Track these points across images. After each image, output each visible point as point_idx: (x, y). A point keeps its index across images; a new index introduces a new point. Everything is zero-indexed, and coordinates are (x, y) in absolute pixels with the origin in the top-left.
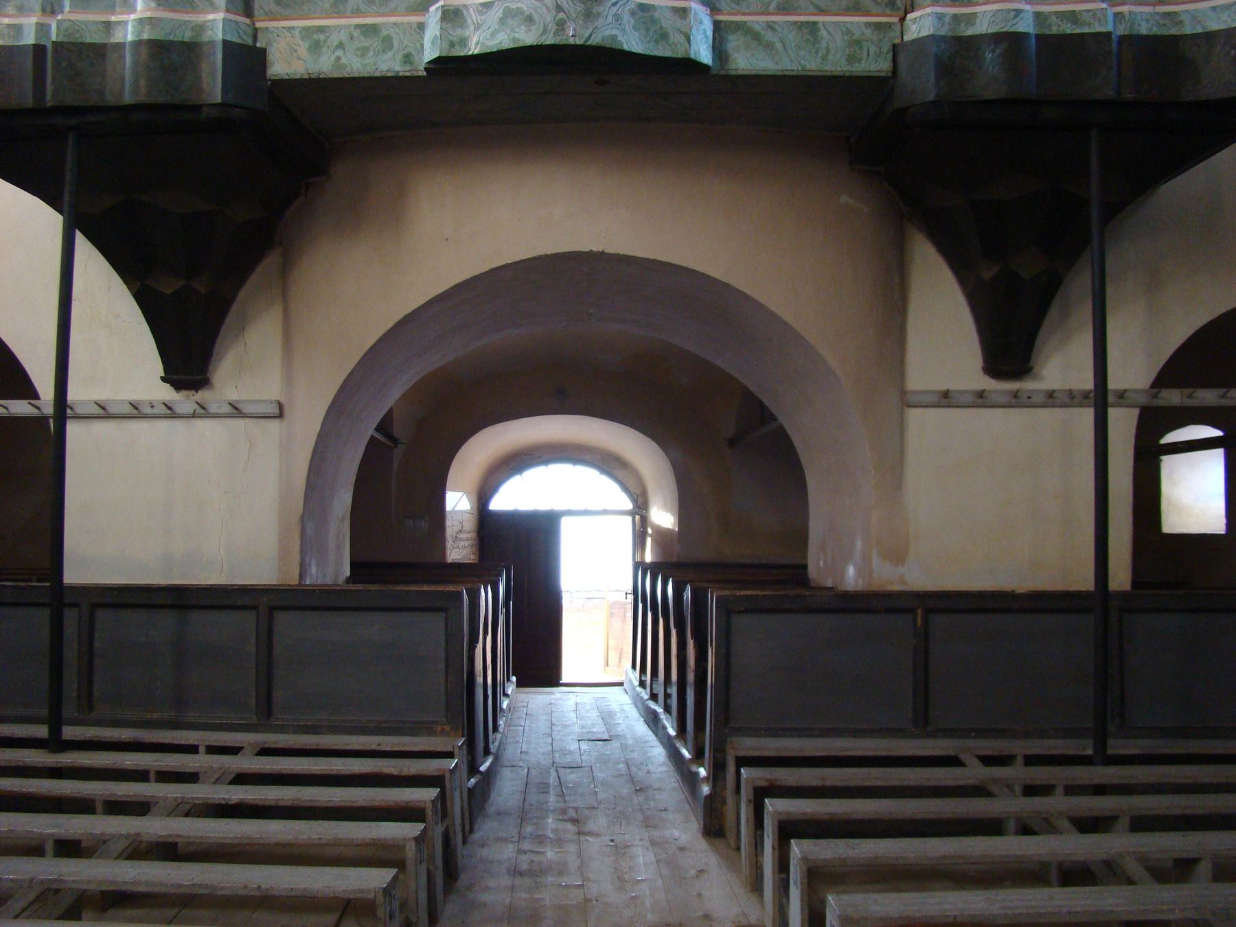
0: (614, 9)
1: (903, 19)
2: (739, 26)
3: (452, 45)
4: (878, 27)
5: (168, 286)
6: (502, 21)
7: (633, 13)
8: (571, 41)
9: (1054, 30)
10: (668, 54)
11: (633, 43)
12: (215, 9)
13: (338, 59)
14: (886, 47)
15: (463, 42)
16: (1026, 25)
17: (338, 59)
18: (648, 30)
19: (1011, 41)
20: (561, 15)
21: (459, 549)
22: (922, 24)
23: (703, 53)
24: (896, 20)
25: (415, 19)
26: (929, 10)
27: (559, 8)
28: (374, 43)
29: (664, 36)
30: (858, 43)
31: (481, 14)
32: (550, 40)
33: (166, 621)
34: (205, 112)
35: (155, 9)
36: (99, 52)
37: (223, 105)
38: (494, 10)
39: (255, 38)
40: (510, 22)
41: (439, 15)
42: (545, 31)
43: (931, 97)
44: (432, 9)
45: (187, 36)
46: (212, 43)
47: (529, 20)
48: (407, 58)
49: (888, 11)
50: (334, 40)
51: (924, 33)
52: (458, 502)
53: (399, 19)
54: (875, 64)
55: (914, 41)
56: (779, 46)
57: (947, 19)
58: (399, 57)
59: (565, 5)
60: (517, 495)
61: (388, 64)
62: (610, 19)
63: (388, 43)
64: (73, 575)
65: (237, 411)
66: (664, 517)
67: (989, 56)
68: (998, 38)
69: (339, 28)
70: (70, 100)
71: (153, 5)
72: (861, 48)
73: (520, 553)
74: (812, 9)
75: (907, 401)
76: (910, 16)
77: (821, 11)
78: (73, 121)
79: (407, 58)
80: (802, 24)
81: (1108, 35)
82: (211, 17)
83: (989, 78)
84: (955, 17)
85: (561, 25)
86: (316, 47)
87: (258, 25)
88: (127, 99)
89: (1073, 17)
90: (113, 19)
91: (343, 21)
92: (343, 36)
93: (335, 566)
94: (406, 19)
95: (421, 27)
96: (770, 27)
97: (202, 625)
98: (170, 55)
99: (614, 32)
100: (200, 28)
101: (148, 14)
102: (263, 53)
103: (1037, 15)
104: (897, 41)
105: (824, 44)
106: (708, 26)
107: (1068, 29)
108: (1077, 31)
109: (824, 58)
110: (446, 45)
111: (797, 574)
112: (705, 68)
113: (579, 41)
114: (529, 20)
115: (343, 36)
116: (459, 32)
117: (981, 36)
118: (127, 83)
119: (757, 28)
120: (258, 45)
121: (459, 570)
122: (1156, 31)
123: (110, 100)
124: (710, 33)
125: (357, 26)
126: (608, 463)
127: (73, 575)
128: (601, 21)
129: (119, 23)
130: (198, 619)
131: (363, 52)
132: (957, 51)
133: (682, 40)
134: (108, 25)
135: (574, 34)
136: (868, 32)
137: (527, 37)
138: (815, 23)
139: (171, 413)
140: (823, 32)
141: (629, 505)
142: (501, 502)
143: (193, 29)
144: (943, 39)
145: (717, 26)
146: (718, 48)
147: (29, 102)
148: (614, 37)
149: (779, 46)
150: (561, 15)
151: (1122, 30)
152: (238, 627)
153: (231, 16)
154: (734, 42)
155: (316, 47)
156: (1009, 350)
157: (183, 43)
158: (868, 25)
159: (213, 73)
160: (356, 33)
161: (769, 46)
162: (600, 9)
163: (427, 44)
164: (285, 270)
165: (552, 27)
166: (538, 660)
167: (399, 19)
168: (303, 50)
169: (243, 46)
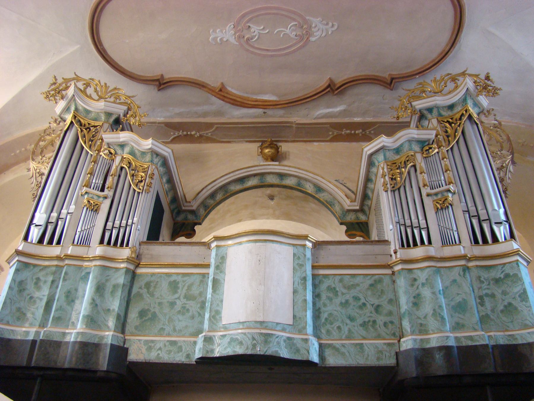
0: (277, 339)
1: (399, 341)
2: (330, 345)
3: (207, 352)
4: (389, 345)
6: (229, 343)
7: (285, 341)
8: (259, 353)
9: (464, 344)
10: (300, 358)
11: (285, 354)
12: (109, 330)
13: (159, 354)
14: (393, 353)
15: (212, 351)
16: (451, 343)
17: (159, 354)
18: (291, 348)
19: (446, 350)
20: (255, 342)
22: (408, 343)
23: (315, 359)
24: (396, 341)
25: (193, 339)
26: (410, 337)
27: (254, 339)
28: (174, 349)
29: (298, 351)
30: (381, 352)
31: (221, 339)
32: (249, 352)
34: (98, 374)
35: (85, 329)
36: (58, 345)
37: (107, 371)
38: (226, 338)
39: (124, 343)
40: (233, 343)
41: (203, 339)
42: (247, 348)
43: (414, 375)
44: (200, 336)
45: (96, 341)
46: (106, 344)
47: (241, 343)
48: (188, 356)
49: (393, 338)
50: (158, 346)
51: (409, 347)
53: (186, 339)
54: (390, 361)
55: (406, 351)
56: (347, 354)
57: (418, 341)
58: (185, 355)
59: (256, 337)
61: (179, 358)
62: (275, 344)
63: (180, 349)
67: (438, 357)
68: (441, 348)
69: (160, 341)
70: (42, 364)
71: (84, 327)
72: (382, 354)
74: (361, 338)
76: (402, 340)
77: (364, 338)
78: (42, 373)
79: (188, 356)
80: (357, 344)
81: (487, 346)
82: (107, 333)
83: (439, 366)
84: (421, 340)
85: (254, 346)
86: (150, 349)
87: (126, 337)
88: (66, 366)
89: (471, 338)
90: (67, 331)
91: (162, 339)
92: (161, 345)
94: (189, 339)
95: (195, 343)
96: (343, 345)
98: (88, 348)
99: (277, 349)
100: (102, 338)
101: (82, 331)
102: (127, 349)
103: (456, 338)
104: (398, 351)
105: (366, 353)
106: (316, 346)
107: (470, 343)
108: (473, 344)
109: (367, 359)
110: (205, 352)
112: (315, 364)
113: (262, 353)
114: (241, 343)
115: (161, 345)
116: (211, 347)
117: (433, 348)
118: (67, 359)
119: (337, 346)
120: (125, 346)
122: (507, 342)
123: (59, 365)
124: (318, 349)
125: (168, 341)
128: (271, 345)
129: (69, 333)
131: (170, 352)
132: (424, 355)
133: (306, 352)
134: (64, 334)
135: (259, 350)
136: (385, 347)
137: (240, 350)
138: (362, 344)
140: (366, 347)
143: (99, 338)
144: (418, 349)
145: (321, 345)
146: (321, 356)
147: (24, 364)
148: (277, 352)
149: (347, 354)
150: (255, 342)
151: (492, 343)
153: (116, 334)
154: (328, 352)
155: (150, 349)
157: (94, 344)
158: (385, 344)
159: (105, 357)
160: (167, 344)
161: (343, 354)
162: (271, 339)
163: (197, 351)
165: (250, 347)
167: (186, 339)
168: (144, 350)
169: (119, 346)
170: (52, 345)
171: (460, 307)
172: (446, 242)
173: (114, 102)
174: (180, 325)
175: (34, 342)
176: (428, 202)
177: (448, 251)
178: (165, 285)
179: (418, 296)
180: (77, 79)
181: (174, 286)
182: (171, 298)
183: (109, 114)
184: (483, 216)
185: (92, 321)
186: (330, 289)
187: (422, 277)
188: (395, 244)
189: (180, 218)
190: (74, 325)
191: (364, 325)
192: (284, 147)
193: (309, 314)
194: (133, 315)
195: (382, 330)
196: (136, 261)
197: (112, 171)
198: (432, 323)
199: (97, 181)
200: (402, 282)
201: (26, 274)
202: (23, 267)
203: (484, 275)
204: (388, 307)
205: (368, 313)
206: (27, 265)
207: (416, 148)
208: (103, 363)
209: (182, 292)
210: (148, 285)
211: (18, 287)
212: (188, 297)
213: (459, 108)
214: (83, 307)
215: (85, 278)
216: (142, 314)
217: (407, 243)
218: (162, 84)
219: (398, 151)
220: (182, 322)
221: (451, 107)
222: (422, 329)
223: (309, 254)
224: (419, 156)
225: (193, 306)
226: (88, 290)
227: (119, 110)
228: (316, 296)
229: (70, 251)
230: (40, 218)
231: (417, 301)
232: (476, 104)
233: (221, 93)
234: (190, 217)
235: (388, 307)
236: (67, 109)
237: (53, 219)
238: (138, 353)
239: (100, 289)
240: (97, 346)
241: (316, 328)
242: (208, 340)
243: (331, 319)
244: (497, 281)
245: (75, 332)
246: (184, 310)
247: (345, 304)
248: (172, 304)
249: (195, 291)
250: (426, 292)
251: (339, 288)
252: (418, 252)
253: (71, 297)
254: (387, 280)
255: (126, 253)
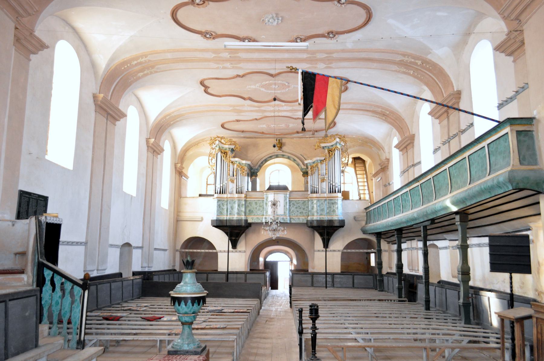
5: (233, 238)
16: (319, 219)
19: (317, 221)
21: (261, 267)
22: (309, 218)
33: (235, 275)
36: (232, 220)
52: (261, 259)
60: (270, 258)
64: (219, 270)
65: (240, 252)
66: (295, 262)
73: (271, 267)
75: (314, 251)
83: (315, 224)
93: (249, 270)
97: (239, 275)
98: (239, 221)
111: (308, 271)
121: (262, 270)
126: (286, 253)
127: (219, 270)
130: (238, 275)
132: (312, 221)
139: (232, 252)
141: (289, 260)
142: (267, 260)
146: (290, 220)
152: (243, 276)
154: (292, 220)
156: (326, 245)
164: (246, 235)
166: (274, 285)
170: (231, 221)
171: (322, 210)
172: (323, 192)
173: (230, 145)
174: (258, 213)
175: (227, 220)
176: (320, 180)
177: (322, 195)
178: (254, 203)
179: (313, 207)
180: (218, 137)
181: (256, 203)
182: (256, 206)
183: (229, 148)
184: (334, 184)
185: (238, 214)
186: (293, 204)
187: (315, 202)
188: (309, 192)
189: (252, 171)
190: (234, 215)
191: (300, 213)
192: (284, 141)
193: (288, 211)
194: (247, 211)
195: (304, 214)
196: (246, 197)
197: (235, 170)
198: (315, 214)
199: (231, 173)
200: (310, 203)
201: (220, 203)
202: (219, 201)
203: (330, 202)
204: (306, 209)
205: (301, 210)
206: (219, 200)
207: (319, 161)
208: (243, 224)
209: (258, 205)
210: (250, 203)
211: (219, 206)
212: (260, 206)
213: (334, 146)
214: (236, 210)
215: (235, 203)
216: (250, 211)
217: (313, 192)
218: (243, 132)
219: (314, 163)
220: (259, 212)
221: (332, 146)
222: (313, 215)
223: (288, 196)
224: (319, 164)
225: (261, 209)
226: (236, 206)
227: (233, 147)
228: (290, 206)
229: (229, 196)
230: (218, 186)
231: (313, 208)
232: (340, 144)
233: (263, 133)
234: (256, 170)
235: (306, 209)
236: (216, 146)
237: (222, 185)
238: (249, 221)
239: (239, 206)
240: (241, 220)
241: (289, 213)
242: (266, 218)
243: (293, 211)
244: (333, 203)
245: (235, 217)
246: (259, 210)
247: (296, 208)
248: (256, 208)
249: (261, 204)
250: (315, 206)
251: (295, 204)
252: (315, 195)
253: (232, 208)
254: (307, 202)
255: (243, 195)
